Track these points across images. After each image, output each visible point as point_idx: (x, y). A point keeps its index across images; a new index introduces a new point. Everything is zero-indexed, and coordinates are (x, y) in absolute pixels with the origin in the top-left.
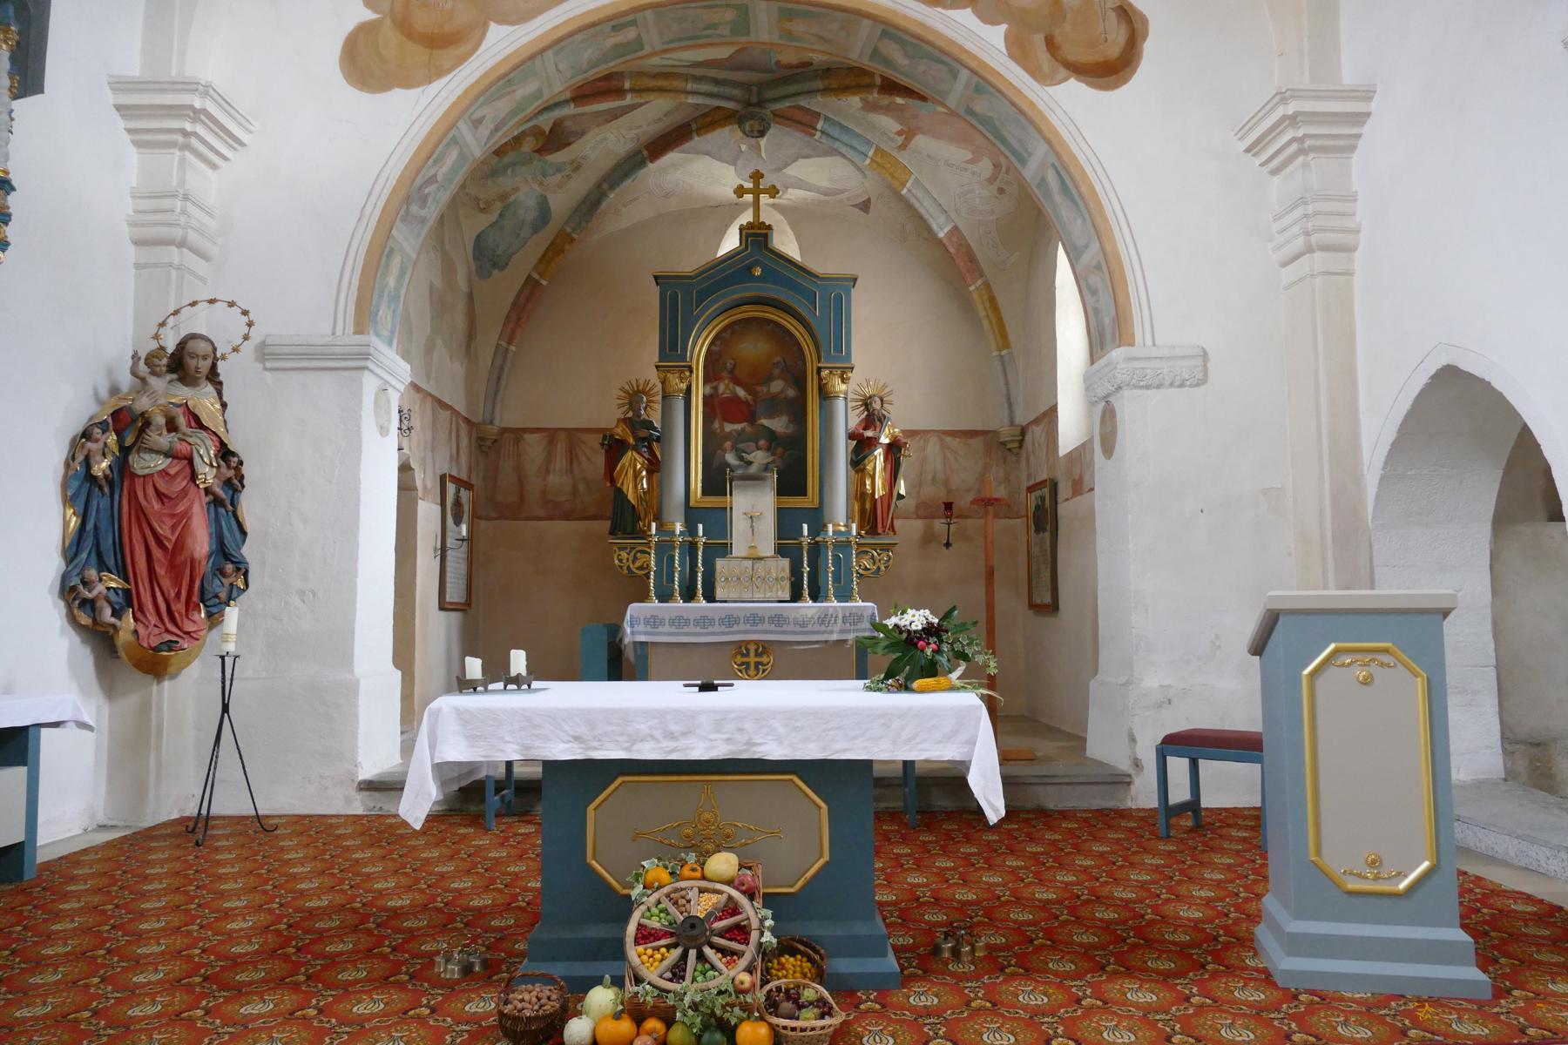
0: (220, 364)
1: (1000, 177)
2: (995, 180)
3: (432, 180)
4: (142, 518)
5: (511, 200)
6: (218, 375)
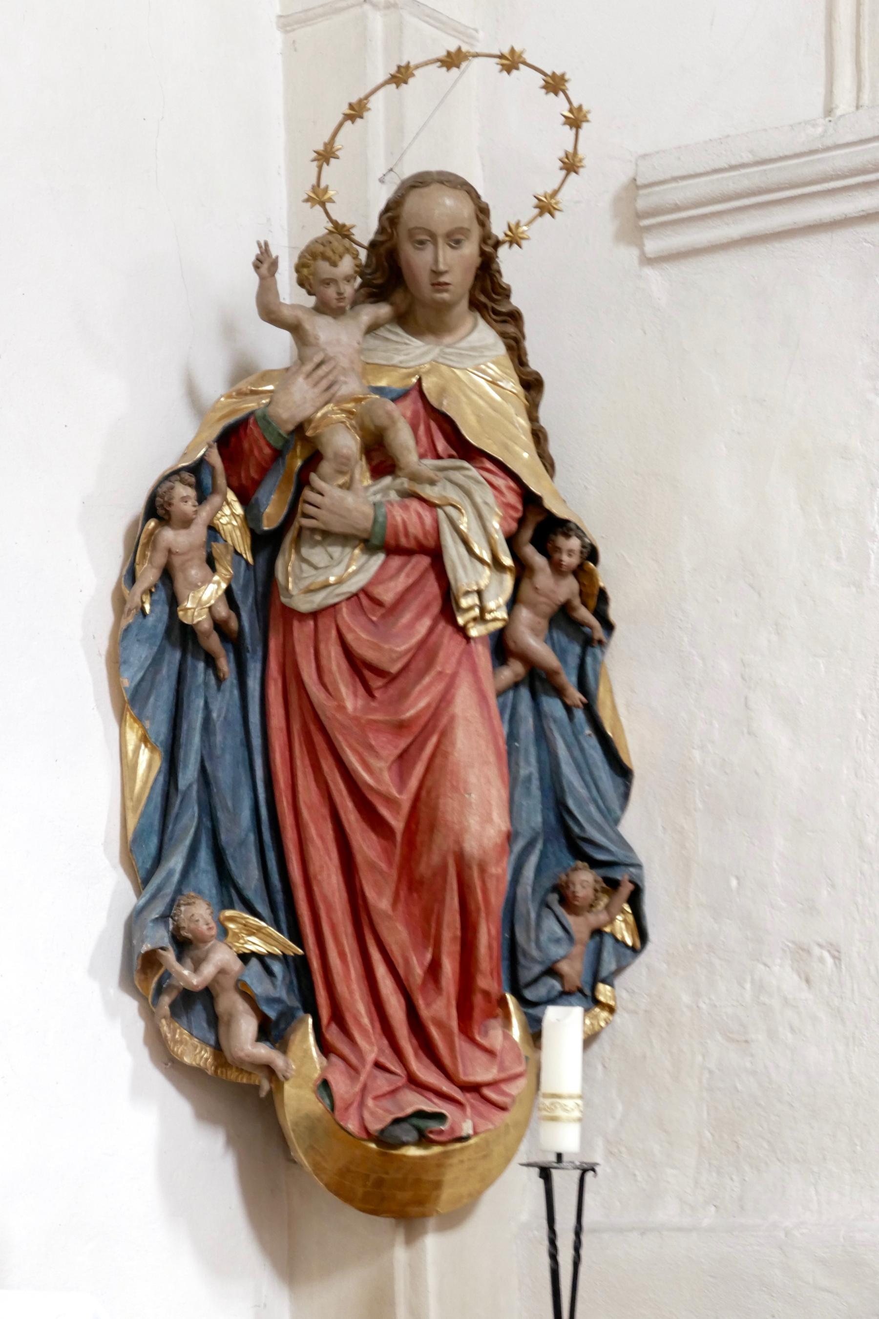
0: (505, 257)
4: (318, 740)
6: (506, 293)
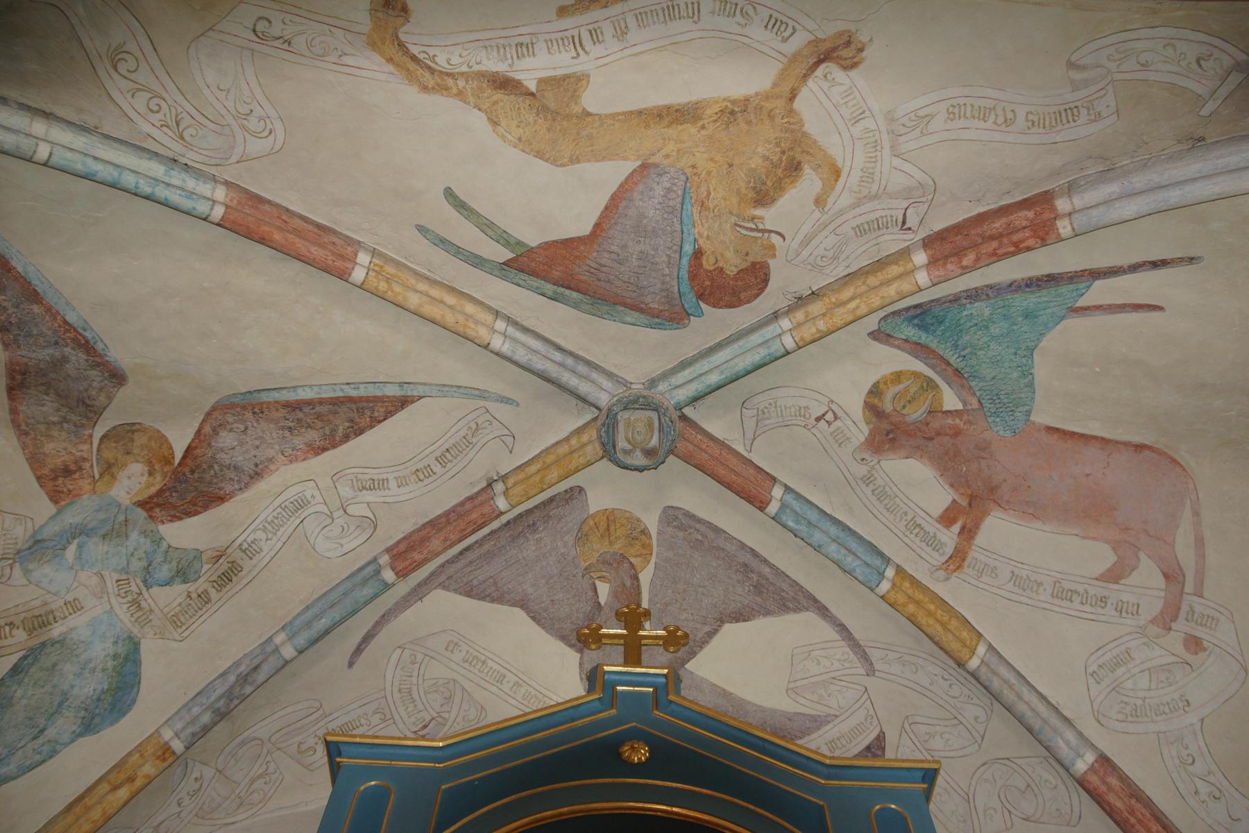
5: (57, 631)
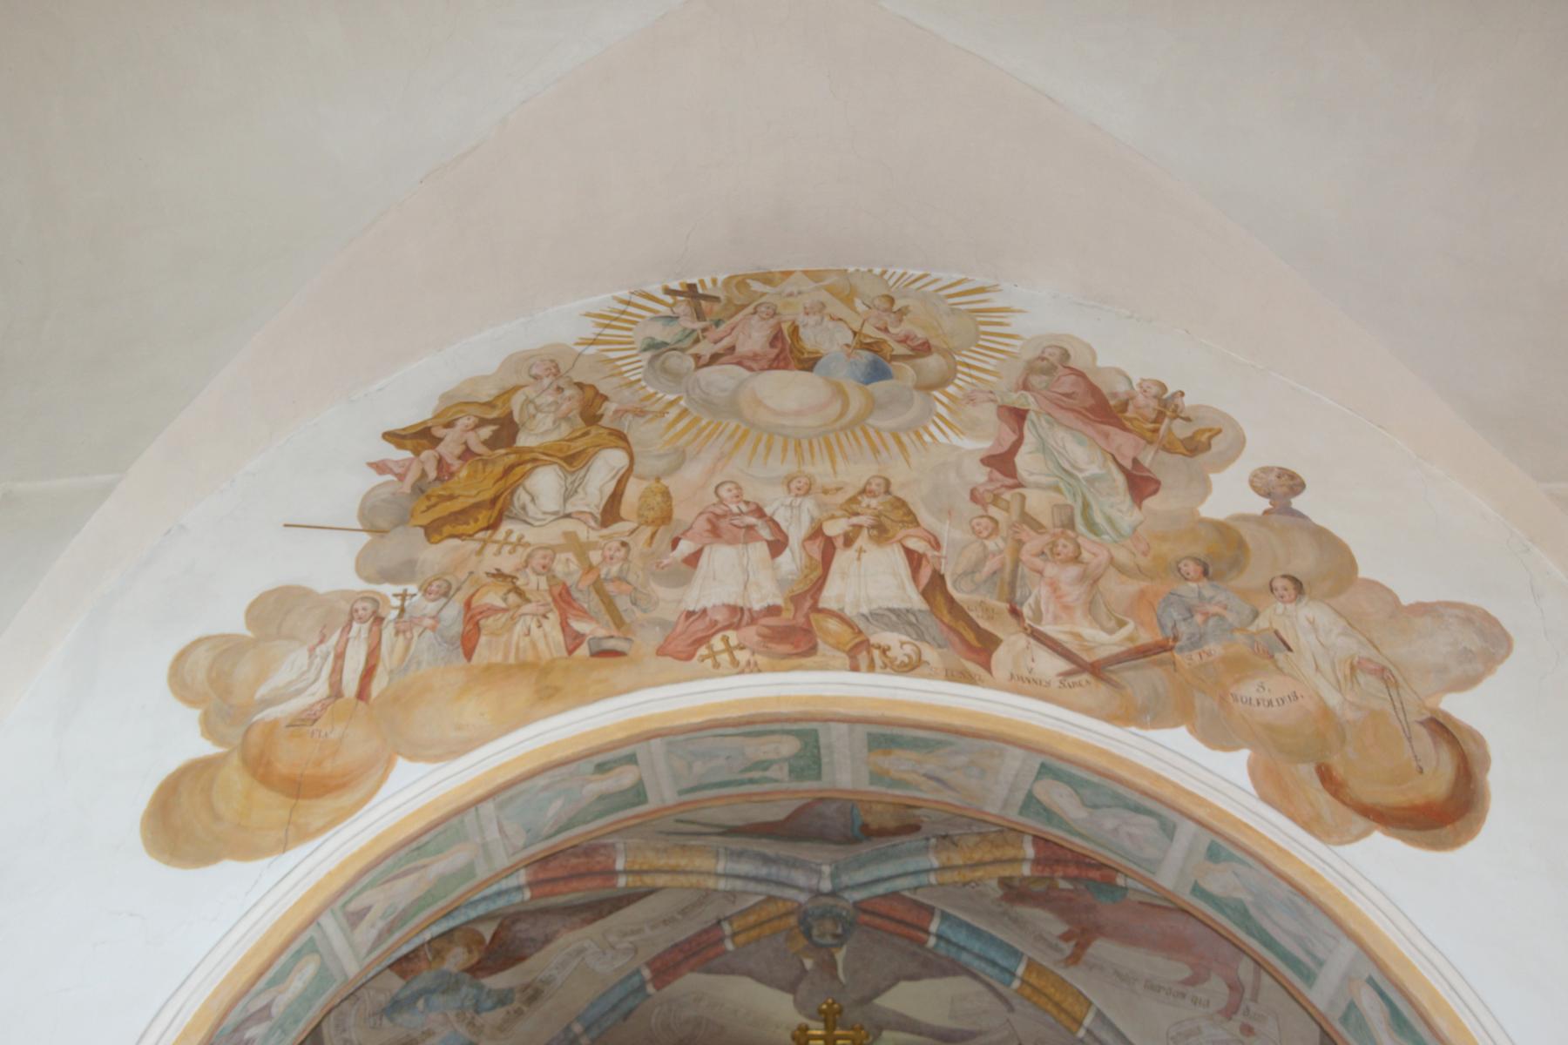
1: (1243, 1007)
2: (1235, 1013)
3: (264, 1013)
